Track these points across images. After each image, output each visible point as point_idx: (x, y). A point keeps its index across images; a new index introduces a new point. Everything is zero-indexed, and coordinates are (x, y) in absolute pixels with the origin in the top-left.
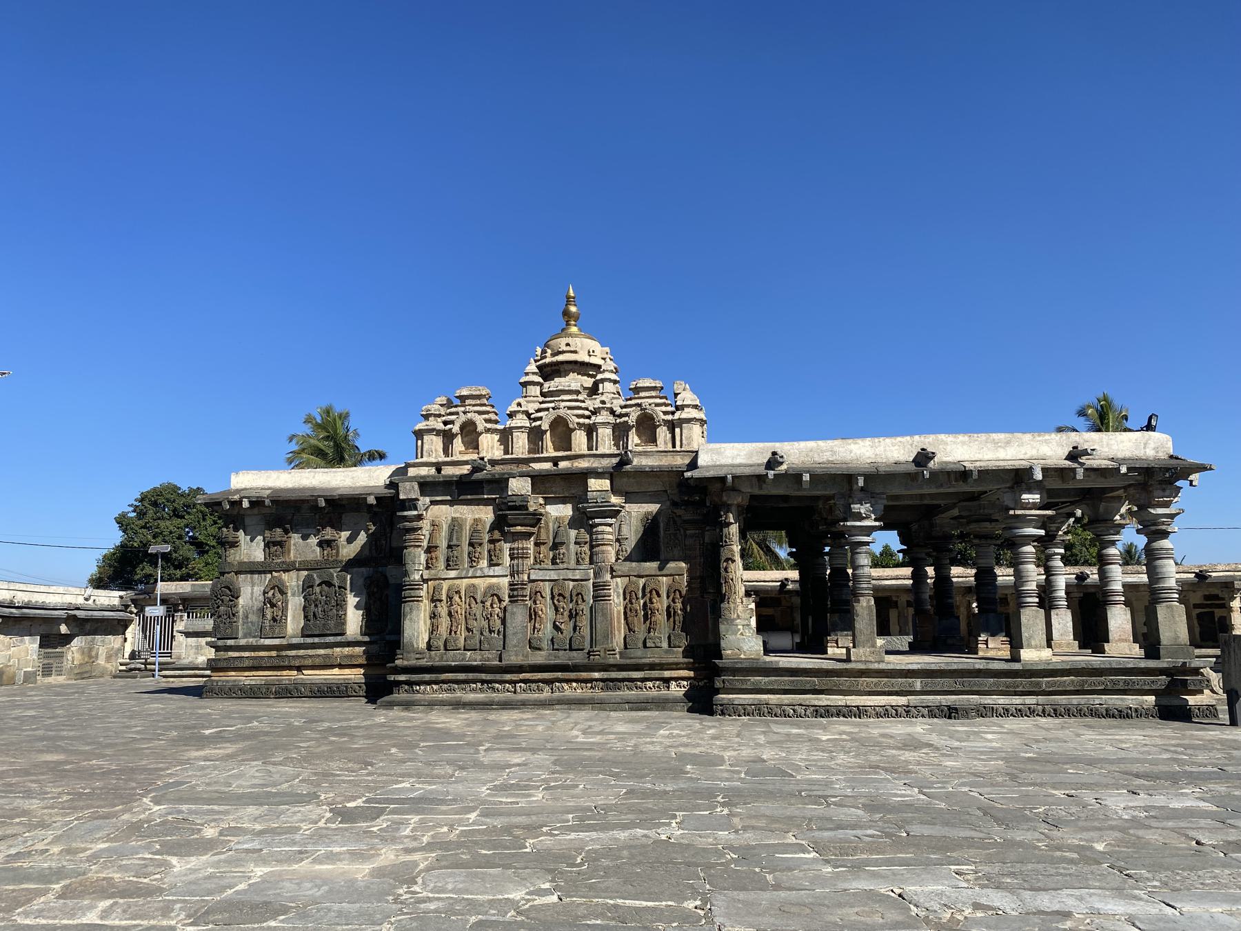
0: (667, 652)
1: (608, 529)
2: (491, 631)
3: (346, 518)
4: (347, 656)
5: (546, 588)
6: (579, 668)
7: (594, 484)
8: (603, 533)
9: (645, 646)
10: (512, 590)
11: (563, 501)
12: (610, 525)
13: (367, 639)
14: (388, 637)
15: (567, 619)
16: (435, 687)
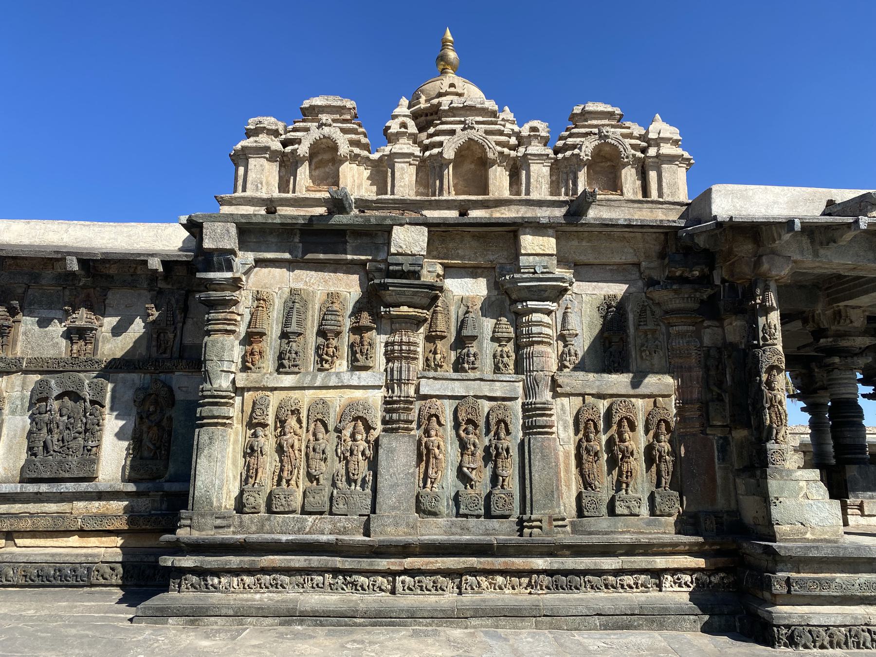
0: (649, 524)
1: (546, 319)
2: (350, 481)
3: (113, 297)
4: (95, 516)
5: (446, 410)
6: (504, 547)
7: (529, 242)
8: (540, 324)
9: (612, 512)
10: (387, 411)
11: (473, 272)
12: (548, 313)
13: (131, 487)
14: (167, 487)
15: (480, 463)
16: (248, 580)
